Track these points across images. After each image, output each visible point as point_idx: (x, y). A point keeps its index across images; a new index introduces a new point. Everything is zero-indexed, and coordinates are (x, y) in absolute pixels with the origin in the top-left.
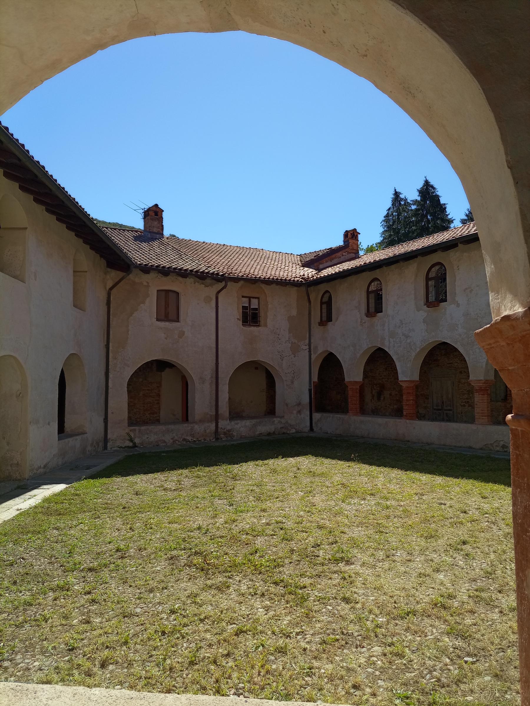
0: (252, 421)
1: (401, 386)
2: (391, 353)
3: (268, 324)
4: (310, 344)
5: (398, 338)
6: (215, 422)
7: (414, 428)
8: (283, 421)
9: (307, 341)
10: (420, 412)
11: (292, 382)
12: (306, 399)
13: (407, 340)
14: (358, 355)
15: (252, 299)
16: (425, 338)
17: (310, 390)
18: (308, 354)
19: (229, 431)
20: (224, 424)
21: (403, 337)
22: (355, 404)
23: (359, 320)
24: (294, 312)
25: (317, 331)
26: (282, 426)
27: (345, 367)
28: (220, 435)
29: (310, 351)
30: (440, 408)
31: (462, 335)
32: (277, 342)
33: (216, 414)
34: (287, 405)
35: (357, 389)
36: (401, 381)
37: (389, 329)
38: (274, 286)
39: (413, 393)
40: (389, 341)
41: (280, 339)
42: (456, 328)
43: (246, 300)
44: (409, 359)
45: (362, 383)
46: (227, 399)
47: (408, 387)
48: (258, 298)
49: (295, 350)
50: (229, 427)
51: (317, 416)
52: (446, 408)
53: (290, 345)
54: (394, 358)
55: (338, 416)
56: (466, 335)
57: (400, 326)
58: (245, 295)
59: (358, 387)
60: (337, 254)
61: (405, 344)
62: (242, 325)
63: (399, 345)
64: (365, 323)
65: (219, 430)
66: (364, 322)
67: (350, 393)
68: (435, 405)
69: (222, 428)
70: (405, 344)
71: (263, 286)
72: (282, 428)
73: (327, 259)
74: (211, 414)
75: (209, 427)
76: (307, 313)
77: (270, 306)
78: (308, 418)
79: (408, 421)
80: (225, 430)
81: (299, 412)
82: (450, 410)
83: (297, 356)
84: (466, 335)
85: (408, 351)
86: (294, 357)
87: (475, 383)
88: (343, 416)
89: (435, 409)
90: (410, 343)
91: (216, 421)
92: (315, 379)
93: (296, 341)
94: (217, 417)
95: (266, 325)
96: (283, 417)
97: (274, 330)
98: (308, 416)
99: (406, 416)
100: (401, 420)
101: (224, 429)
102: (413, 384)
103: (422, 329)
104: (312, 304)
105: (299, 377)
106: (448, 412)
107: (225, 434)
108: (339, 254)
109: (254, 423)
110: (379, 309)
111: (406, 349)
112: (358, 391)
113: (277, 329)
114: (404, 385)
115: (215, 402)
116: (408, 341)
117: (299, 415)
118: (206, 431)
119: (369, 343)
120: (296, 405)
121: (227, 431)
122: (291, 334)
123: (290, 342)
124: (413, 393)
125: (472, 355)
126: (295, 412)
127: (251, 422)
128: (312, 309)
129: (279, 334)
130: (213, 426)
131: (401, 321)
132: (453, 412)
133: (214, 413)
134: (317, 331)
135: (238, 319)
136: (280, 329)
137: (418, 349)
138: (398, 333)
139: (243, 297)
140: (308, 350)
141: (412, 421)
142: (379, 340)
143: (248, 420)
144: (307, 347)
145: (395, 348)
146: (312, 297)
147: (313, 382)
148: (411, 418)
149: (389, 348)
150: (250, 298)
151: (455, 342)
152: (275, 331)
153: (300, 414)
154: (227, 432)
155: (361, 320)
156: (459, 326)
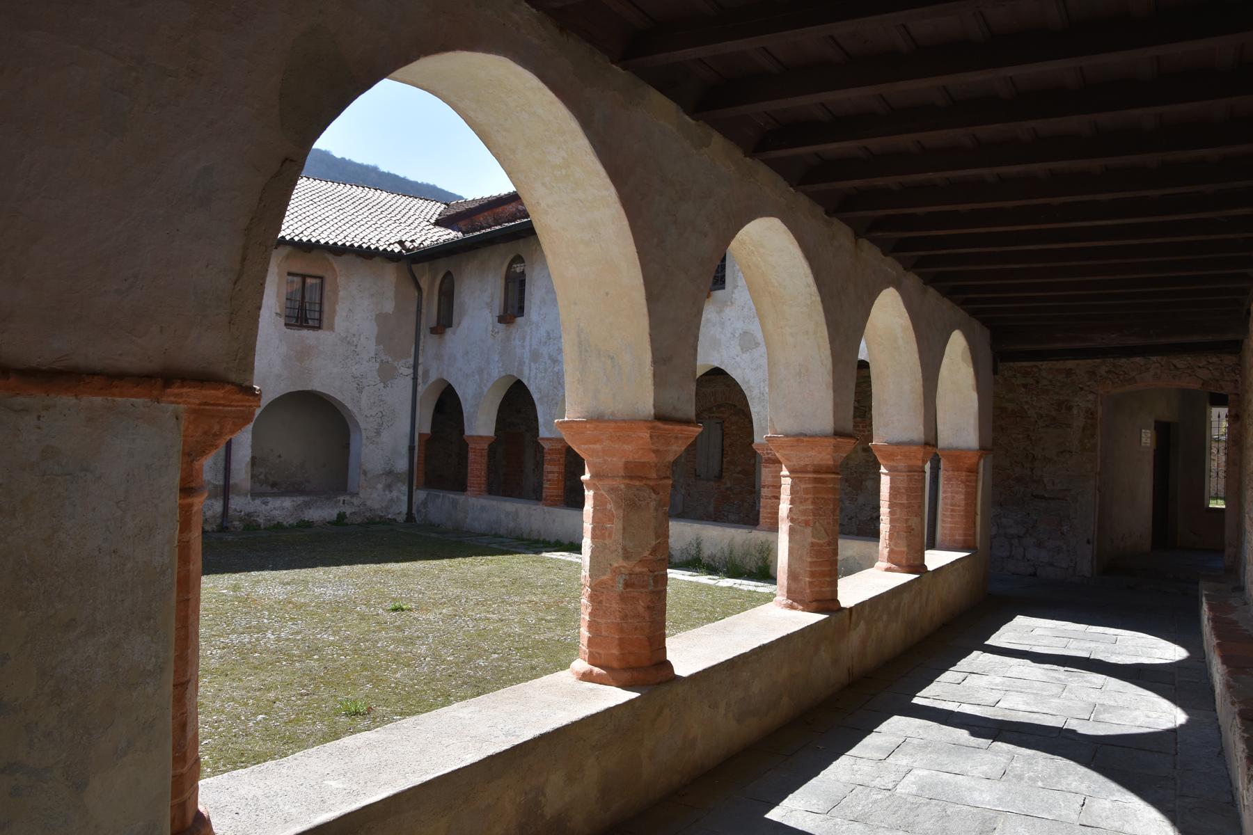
0: (295, 499)
2: (532, 389)
3: (336, 326)
4: (415, 367)
6: (222, 497)
8: (355, 501)
9: (411, 361)
11: (378, 433)
12: (402, 465)
14: (486, 390)
15: (309, 281)
17: (411, 449)
18: (411, 383)
19: (249, 515)
20: (238, 503)
21: (549, 361)
22: (478, 477)
23: (490, 328)
24: (389, 307)
25: (428, 342)
26: (353, 511)
27: (467, 408)
28: (231, 522)
29: (415, 379)
32: (352, 360)
33: (225, 485)
34: (365, 473)
35: (483, 449)
37: (531, 346)
38: (345, 257)
39: (559, 460)
40: (530, 367)
41: (358, 355)
43: (298, 280)
45: (493, 440)
46: (248, 459)
47: (551, 450)
48: (322, 278)
49: (386, 374)
50: (250, 509)
51: (420, 495)
53: (377, 365)
54: (535, 397)
55: (451, 496)
57: (546, 343)
58: (294, 270)
59: (486, 446)
60: (506, 207)
62: (286, 325)
63: (543, 374)
64: (498, 332)
65: (231, 512)
66: (496, 330)
67: (471, 456)
69: (235, 510)
71: (331, 257)
72: (354, 513)
73: (486, 214)
74: (217, 483)
75: (212, 506)
76: (414, 309)
77: (342, 293)
78: (405, 498)
79: (546, 508)
80: (243, 513)
81: (389, 487)
83: (389, 385)
86: (384, 387)
88: (457, 497)
90: (558, 373)
91: (225, 497)
92: (425, 427)
93: (390, 359)
94: (226, 491)
95: (331, 328)
96: (357, 494)
97: (347, 337)
98: (405, 495)
99: (545, 500)
100: (538, 507)
101: (241, 511)
102: (561, 445)
104: (425, 295)
105: (392, 425)
107: (241, 520)
108: (511, 207)
109: (299, 503)
110: (521, 311)
112: (485, 453)
113: (354, 335)
114: (546, 446)
115: (223, 463)
117: (387, 493)
118: (205, 513)
120: (383, 474)
121: (245, 515)
122: (382, 346)
123: (379, 360)
124: (559, 460)
126: (380, 486)
127: (293, 501)
128: (424, 303)
129: (356, 346)
130: (218, 506)
131: (548, 333)
133: (222, 483)
134: (428, 342)
135: (277, 314)
136: (360, 335)
138: (542, 354)
139: (289, 274)
140: (412, 375)
141: (551, 509)
142: (516, 364)
143: (287, 498)
144: (411, 371)
146: (424, 283)
147: (419, 434)
148: (554, 504)
149: (529, 380)
150: (304, 277)
152: (348, 339)
153: (391, 491)
154: (246, 517)
155: (493, 327)
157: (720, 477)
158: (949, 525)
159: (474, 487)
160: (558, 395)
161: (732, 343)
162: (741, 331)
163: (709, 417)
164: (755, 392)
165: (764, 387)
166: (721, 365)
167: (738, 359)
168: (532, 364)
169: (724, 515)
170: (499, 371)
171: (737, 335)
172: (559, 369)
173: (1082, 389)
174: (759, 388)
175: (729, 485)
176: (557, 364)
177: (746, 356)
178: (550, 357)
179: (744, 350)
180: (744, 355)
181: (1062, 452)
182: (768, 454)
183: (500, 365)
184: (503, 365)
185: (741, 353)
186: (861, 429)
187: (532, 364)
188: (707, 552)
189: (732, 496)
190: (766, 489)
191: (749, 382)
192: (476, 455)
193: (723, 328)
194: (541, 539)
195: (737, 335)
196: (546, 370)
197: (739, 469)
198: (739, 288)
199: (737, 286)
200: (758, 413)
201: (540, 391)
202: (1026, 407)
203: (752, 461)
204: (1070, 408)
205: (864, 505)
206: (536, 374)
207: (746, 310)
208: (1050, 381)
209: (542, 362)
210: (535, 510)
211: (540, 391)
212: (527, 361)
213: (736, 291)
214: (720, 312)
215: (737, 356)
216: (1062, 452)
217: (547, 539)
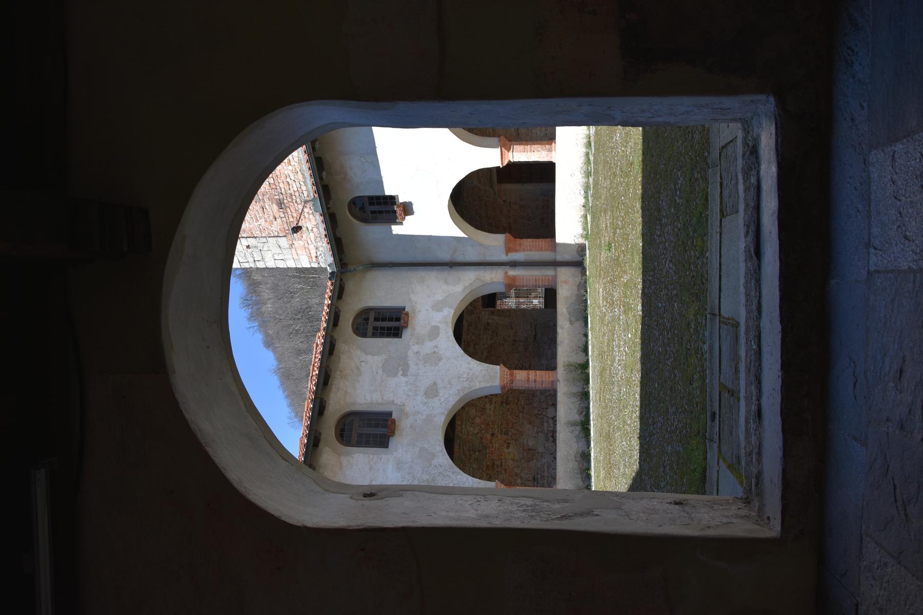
158: (543, 243)
161: (430, 405)
162: (424, 398)
164: (466, 385)
165: (463, 378)
167: (442, 399)
171: (426, 400)
173: (479, 318)
174: (463, 381)
177: (441, 392)
179: (437, 394)
180: (440, 395)
181: (511, 326)
182: (507, 375)
185: (438, 398)
186: (493, 449)
188: (577, 418)
190: (530, 376)
191: (458, 390)
193: (420, 413)
195: (426, 400)
198: (394, 399)
199: (393, 401)
200: (480, 382)
202: (486, 346)
204: (488, 323)
205: (545, 447)
207: (410, 393)
208: (473, 334)
213: (396, 402)
214: (407, 415)
215: (440, 400)
216: (511, 326)
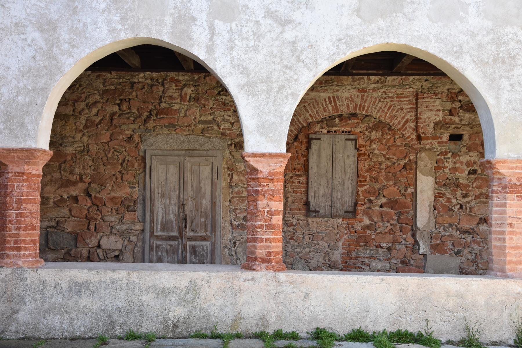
1: (254, 171)
5: (250, 24)
7: (307, 296)
10: (104, 246)
13: (282, 32)
16: (351, 33)
21: (268, 21)
30: (175, 234)
31: (480, 36)
36: (254, 155)
40: (212, 29)
42: (461, 13)
44: (290, 91)
52: (192, 234)
56: (491, 36)
61: (277, 43)
63: (252, 43)
68: (159, 226)
70: (277, 43)
79: (283, 276)
82: (204, 239)
84: (491, 36)
85: (286, 67)
87: (512, 168)
89: (158, 238)
90: (294, 43)
103: (343, 6)
106: (198, 243)
111: (277, 60)
116: (289, 35)
119: (120, 27)
125: (508, 91)
132: (213, 245)
137: (326, 62)
138: (246, 7)
142: (168, 20)
145: (235, 54)
149: (210, 49)
151: (456, 52)
156: (472, 9)
157: (353, 213)
159: (26, 249)
160: (296, 80)
163: (328, 132)
166: (459, 55)
168: (219, 24)
169: (362, 262)
170: (112, 30)
172: (296, 37)
175: (367, 221)
176: (290, 26)
178: (269, 14)
183: (116, 18)
184: (123, 19)
187: (219, 24)
189: (373, 237)
192: (30, 187)
194: (271, 331)
196: (258, 36)
197: (384, 200)
201: (245, 72)
203: (411, 190)
206: (230, 41)
209: (247, 21)
210: (253, 279)
211: (245, 72)
212: (202, 18)
217: (287, 329)
